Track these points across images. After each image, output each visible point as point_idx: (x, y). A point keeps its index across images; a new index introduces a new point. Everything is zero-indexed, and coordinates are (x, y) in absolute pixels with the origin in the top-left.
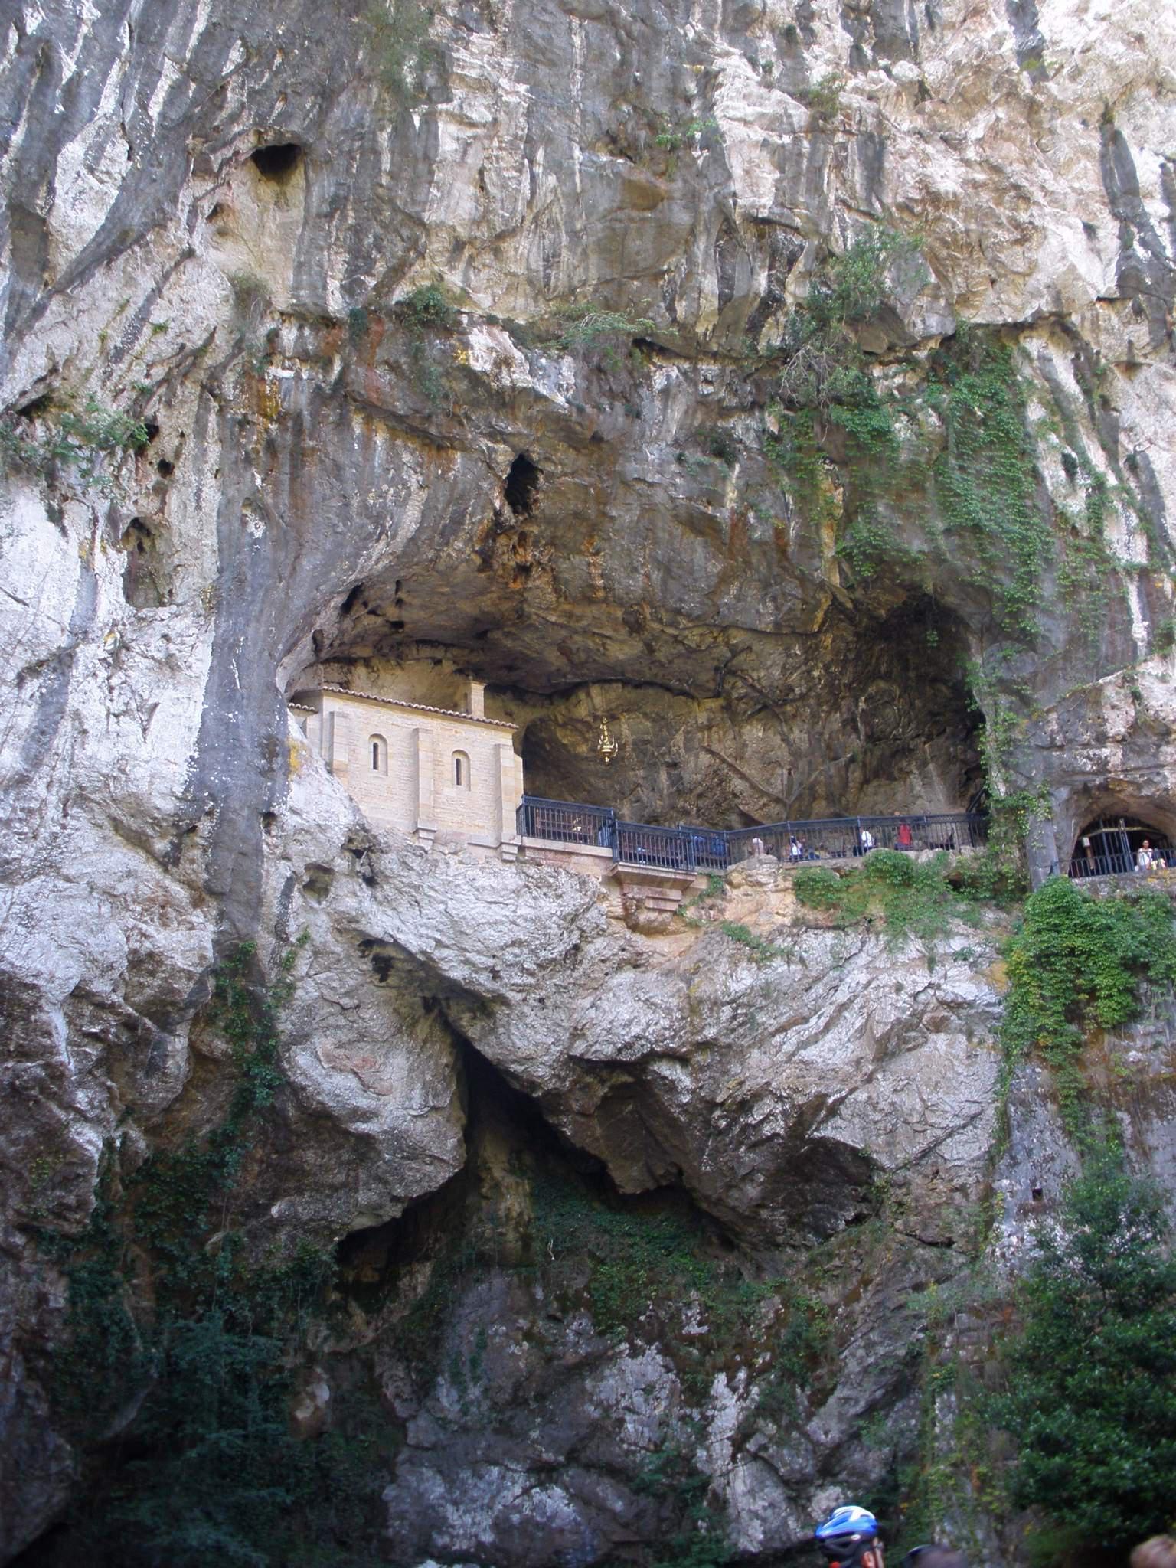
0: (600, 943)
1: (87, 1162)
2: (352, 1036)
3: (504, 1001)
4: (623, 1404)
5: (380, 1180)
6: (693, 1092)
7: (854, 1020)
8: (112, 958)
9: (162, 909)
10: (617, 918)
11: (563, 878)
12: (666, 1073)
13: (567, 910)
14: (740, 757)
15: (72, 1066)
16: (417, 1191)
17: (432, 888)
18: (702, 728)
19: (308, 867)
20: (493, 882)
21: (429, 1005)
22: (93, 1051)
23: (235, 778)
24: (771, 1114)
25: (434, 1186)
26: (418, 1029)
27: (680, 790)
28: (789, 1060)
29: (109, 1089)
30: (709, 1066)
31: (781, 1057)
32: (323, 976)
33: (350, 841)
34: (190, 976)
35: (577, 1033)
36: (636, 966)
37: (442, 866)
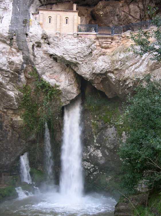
0: (95, 51)
1: (12, 97)
2: (53, 72)
3: (79, 64)
4: (109, 136)
5: (64, 97)
6: (115, 79)
7: (145, 63)
8: (5, 63)
9: (11, 53)
10: (98, 46)
11: (86, 39)
12: (110, 75)
13: (87, 45)
14: (130, 12)
15: (4, 82)
16: (71, 99)
17: (60, 44)
18: (121, 7)
19: (36, 43)
20: (72, 41)
21: (68, 65)
22: (8, 79)
23: (19, 28)
24: (130, 82)
25: (74, 98)
26: (67, 70)
27: (120, 20)
28: (133, 72)
29: (13, 85)
30: (117, 73)
31: (131, 71)
32: (44, 62)
33: (43, 37)
34: (20, 65)
35: (93, 69)
36: (104, 55)
37: (62, 39)
